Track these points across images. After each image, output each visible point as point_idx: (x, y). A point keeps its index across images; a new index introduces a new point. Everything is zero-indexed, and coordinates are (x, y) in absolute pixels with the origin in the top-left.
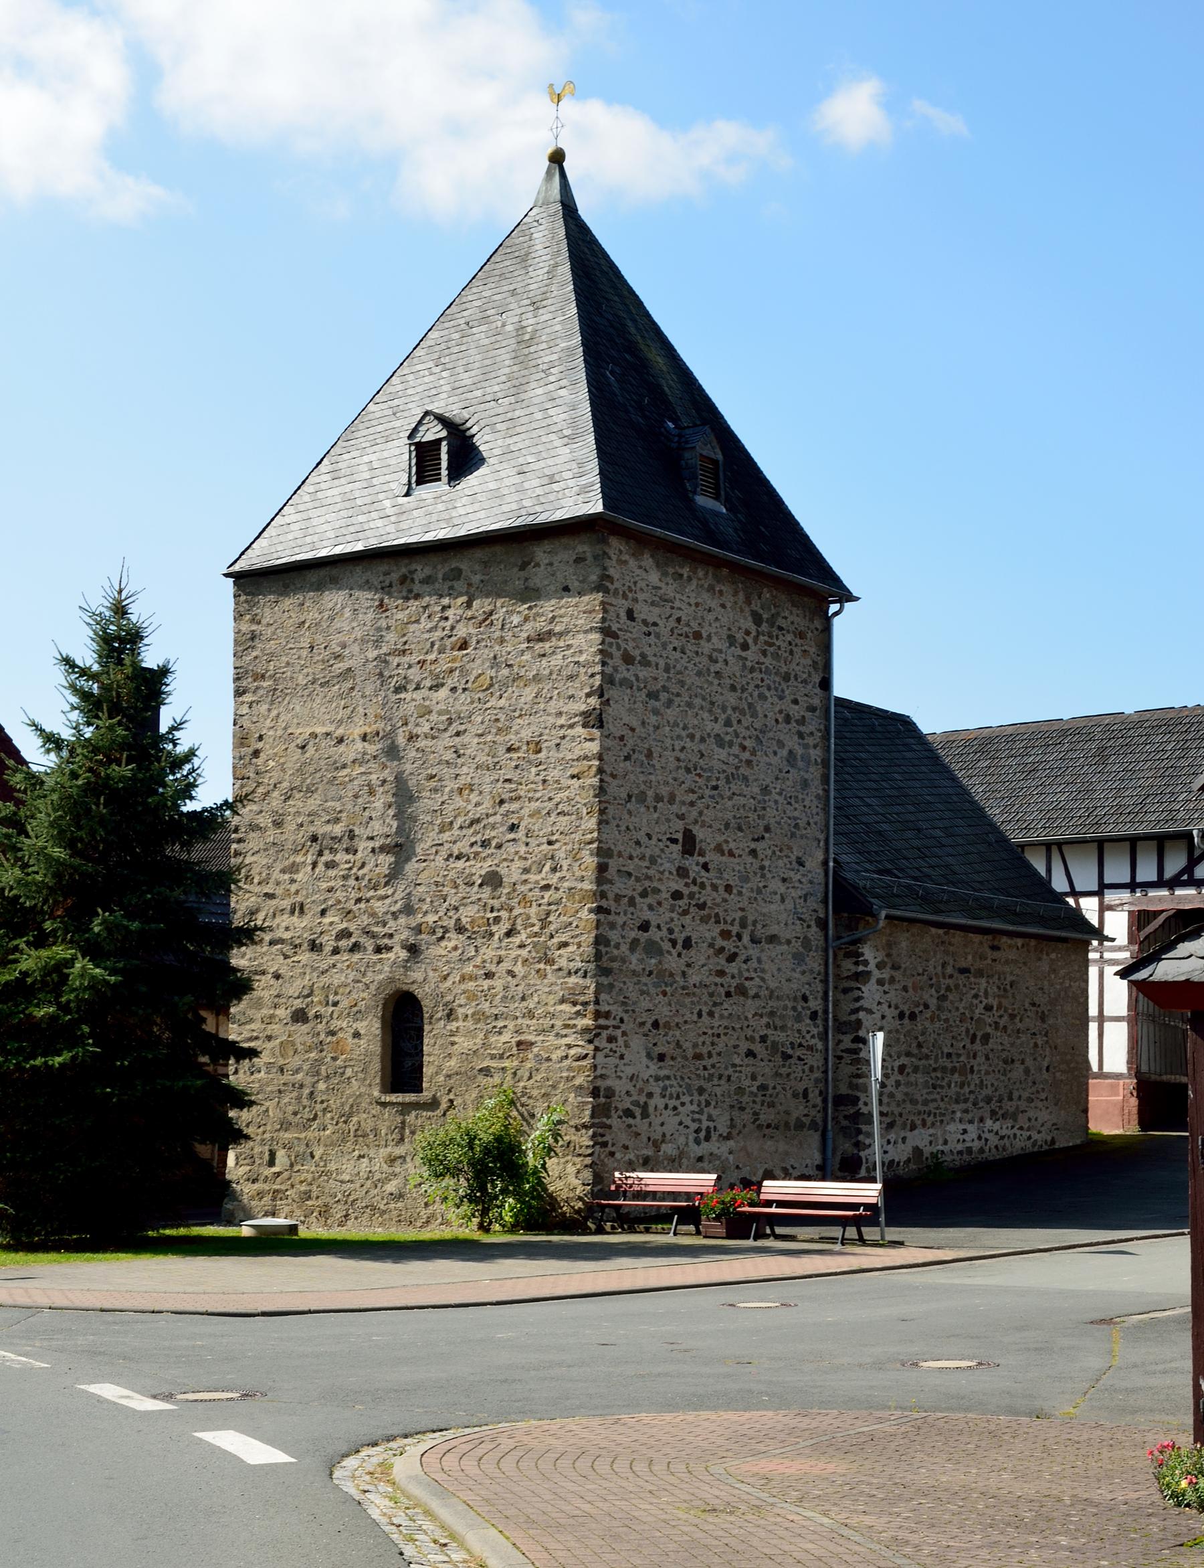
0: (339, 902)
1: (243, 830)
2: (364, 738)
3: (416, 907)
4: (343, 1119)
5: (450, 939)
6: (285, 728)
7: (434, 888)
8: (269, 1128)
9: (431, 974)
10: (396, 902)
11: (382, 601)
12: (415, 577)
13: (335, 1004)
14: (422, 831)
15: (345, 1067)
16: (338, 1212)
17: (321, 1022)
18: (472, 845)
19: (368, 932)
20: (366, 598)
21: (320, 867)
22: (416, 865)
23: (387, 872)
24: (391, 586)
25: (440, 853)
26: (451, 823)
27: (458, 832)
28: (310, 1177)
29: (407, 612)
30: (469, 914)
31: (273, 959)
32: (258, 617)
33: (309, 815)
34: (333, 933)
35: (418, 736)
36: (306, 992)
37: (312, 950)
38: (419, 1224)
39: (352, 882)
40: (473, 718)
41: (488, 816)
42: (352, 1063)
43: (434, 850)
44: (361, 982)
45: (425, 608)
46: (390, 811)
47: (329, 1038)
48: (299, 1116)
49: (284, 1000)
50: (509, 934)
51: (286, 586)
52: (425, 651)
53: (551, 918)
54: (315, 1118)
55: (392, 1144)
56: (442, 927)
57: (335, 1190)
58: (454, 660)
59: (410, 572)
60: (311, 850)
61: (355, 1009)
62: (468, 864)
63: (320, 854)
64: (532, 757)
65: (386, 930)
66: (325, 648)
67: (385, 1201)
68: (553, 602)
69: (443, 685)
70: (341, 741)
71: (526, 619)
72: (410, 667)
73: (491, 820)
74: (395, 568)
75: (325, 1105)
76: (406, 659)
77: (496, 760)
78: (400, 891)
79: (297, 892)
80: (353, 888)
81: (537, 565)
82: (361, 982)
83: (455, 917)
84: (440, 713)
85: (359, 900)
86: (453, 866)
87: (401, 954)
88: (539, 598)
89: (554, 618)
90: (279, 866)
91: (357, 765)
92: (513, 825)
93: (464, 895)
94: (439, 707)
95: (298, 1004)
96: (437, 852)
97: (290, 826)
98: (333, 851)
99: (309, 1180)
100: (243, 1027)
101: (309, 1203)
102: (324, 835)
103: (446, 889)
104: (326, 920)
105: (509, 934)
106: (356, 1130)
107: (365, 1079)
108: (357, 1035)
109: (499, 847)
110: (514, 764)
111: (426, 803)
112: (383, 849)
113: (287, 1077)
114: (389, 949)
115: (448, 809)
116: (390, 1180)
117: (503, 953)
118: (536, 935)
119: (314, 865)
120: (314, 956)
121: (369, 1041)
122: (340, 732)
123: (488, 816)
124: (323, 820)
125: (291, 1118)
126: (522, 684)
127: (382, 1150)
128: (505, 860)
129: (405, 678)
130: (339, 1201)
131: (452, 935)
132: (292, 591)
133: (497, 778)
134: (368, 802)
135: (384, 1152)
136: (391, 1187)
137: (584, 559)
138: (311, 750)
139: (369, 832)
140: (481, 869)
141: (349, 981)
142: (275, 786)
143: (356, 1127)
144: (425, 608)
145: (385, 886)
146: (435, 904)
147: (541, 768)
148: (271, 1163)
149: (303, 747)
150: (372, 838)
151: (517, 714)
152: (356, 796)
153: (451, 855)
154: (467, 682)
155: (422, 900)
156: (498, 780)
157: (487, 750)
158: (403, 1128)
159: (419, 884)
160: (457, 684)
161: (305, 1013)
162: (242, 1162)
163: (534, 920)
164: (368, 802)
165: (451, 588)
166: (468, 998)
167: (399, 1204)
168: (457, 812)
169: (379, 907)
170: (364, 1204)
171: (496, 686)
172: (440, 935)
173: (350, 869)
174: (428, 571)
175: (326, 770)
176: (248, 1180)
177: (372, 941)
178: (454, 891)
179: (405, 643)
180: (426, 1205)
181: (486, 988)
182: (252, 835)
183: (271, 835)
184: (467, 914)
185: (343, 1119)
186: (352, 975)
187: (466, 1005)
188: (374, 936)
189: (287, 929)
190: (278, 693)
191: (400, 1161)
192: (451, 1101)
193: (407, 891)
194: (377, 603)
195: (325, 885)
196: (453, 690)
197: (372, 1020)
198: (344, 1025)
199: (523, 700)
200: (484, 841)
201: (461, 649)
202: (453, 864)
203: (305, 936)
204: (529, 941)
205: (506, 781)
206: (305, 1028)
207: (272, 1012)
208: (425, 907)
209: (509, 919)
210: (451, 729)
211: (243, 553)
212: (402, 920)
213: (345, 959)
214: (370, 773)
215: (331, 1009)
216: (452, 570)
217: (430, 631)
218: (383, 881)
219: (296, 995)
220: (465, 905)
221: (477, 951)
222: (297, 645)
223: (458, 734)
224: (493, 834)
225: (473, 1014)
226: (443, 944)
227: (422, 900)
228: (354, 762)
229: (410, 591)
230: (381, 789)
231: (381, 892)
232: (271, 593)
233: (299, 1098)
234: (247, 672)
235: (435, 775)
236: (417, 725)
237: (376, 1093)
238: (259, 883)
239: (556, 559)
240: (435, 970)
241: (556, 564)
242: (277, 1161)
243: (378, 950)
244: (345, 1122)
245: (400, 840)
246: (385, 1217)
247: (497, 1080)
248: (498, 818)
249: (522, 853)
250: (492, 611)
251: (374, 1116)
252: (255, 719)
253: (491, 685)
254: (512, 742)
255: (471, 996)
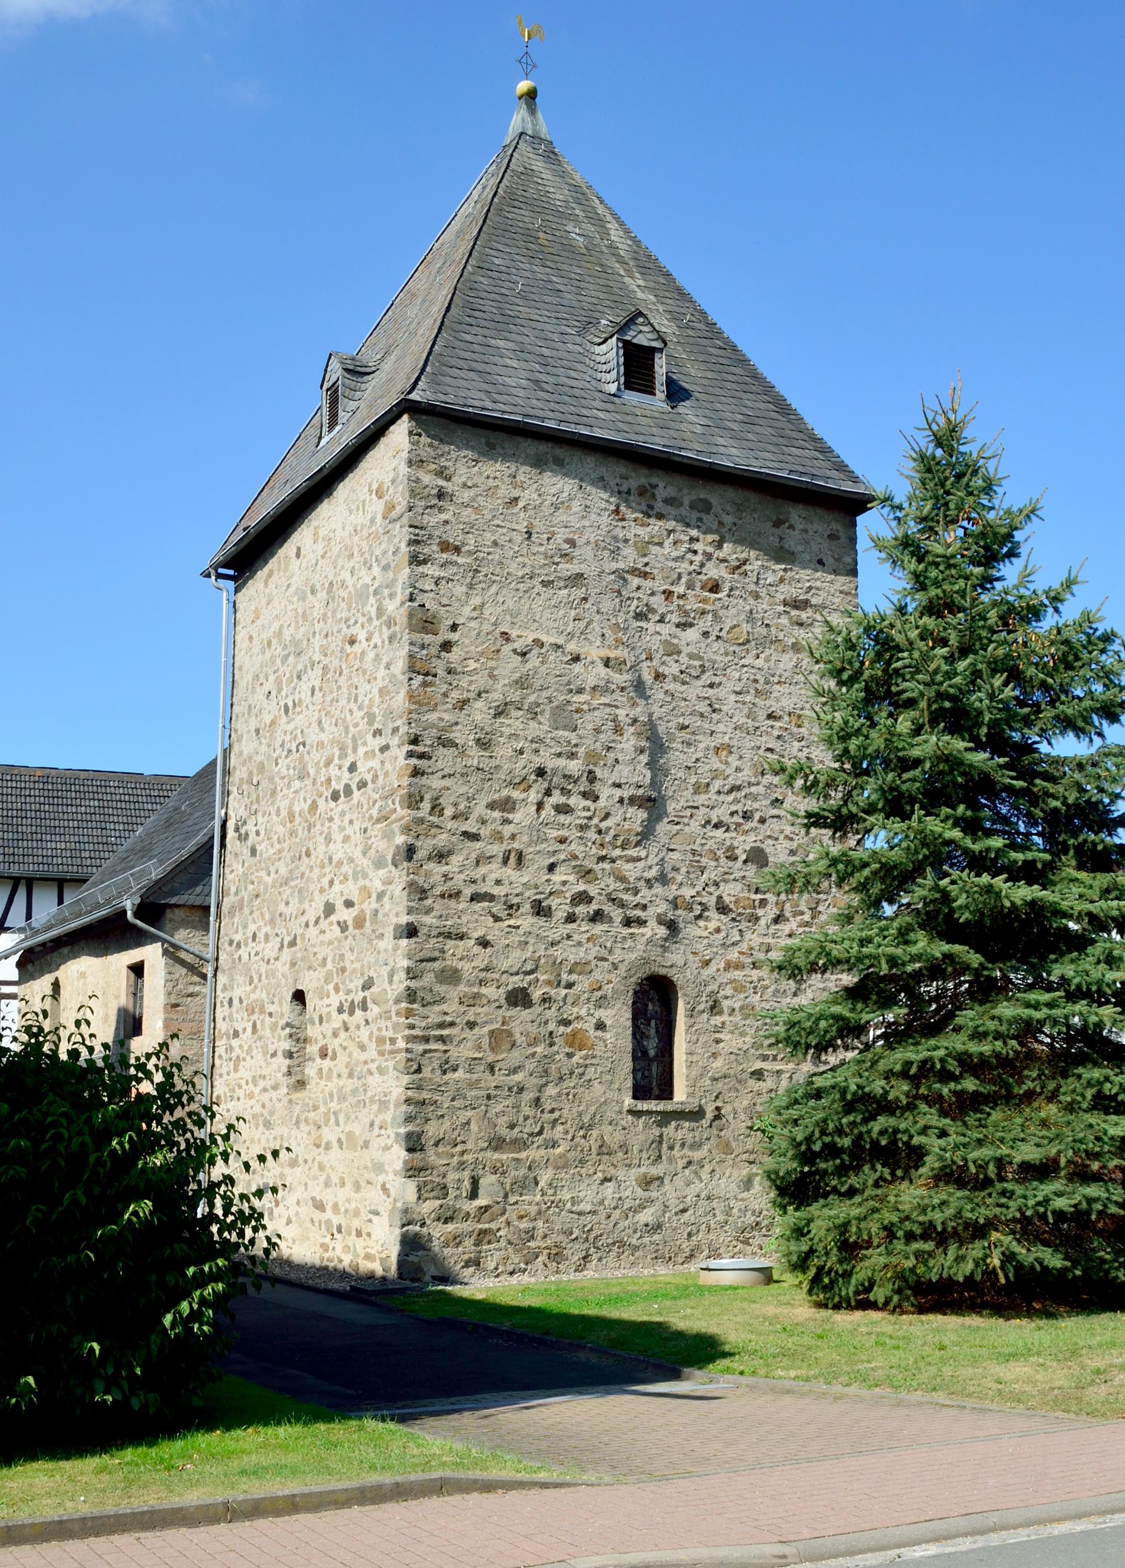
0: (576, 857)
1: (429, 743)
2: (607, 663)
3: (670, 876)
4: (582, 1133)
5: (707, 919)
6: (495, 624)
7: (690, 857)
8: (470, 1145)
9: (691, 957)
10: (650, 867)
11: (618, 506)
12: (656, 492)
13: (570, 986)
14: (674, 788)
15: (586, 1066)
16: (574, 1254)
17: (550, 1008)
18: (732, 814)
19: (614, 900)
20: (600, 498)
21: (548, 811)
22: (669, 827)
23: (640, 829)
24: (629, 492)
25: (695, 817)
26: (708, 785)
27: (715, 797)
28: (533, 1210)
29: (648, 529)
30: (732, 893)
31: (477, 921)
32: (448, 472)
33: (532, 741)
34: (568, 895)
35: (665, 676)
36: (529, 967)
37: (538, 914)
38: (680, 1260)
39: (592, 835)
40: (728, 671)
41: (750, 784)
42: (594, 1061)
43: (688, 812)
44: (607, 960)
45: (670, 532)
46: (641, 757)
47: (562, 1029)
48: (517, 1130)
49: (494, 976)
50: (777, 920)
51: (491, 446)
52: (670, 580)
53: (820, 908)
54: (540, 1133)
55: (647, 1162)
56: (700, 904)
57: (569, 1225)
58: (704, 601)
59: (651, 485)
60: (535, 787)
61: (598, 994)
62: (727, 835)
63: (548, 793)
64: (795, 730)
65: (638, 899)
66: (549, 539)
67: (639, 1234)
68: (809, 572)
69: (691, 625)
70: (576, 659)
71: (782, 580)
72: (653, 594)
73: (753, 789)
74: (633, 475)
75: (556, 1114)
76: (648, 584)
77: (757, 725)
78: (652, 853)
79: (513, 837)
80: (594, 843)
81: (791, 527)
82: (607, 960)
83: (717, 894)
84: (691, 656)
85: (602, 859)
86: (711, 834)
87: (657, 931)
88: (792, 562)
89: (810, 588)
90: (484, 800)
91: (598, 694)
92: (777, 800)
93: (726, 870)
94: (690, 649)
95: (516, 982)
96: (691, 816)
97: (503, 751)
98: (565, 791)
99: (533, 1214)
100: (429, 1008)
101: (532, 1244)
102: (555, 771)
103: (703, 860)
104: (557, 878)
105: (777, 920)
106: (601, 1147)
107: (612, 1082)
108: (600, 1026)
109: (762, 821)
110: (776, 733)
111: (677, 757)
112: (632, 800)
113: (500, 1078)
114: (641, 923)
115: (703, 768)
116: (644, 1208)
117: (771, 940)
118: (807, 924)
119: (540, 806)
120: (541, 921)
121: (618, 1034)
122: (572, 647)
123: (750, 784)
124: (553, 751)
125: (504, 1132)
126: (780, 649)
127: (633, 1171)
128: (769, 837)
129: (647, 605)
130: (576, 1238)
131: (712, 914)
132: (501, 455)
133: (758, 744)
134: (614, 741)
135: (634, 1172)
136: (646, 1216)
137: (838, 538)
138: (534, 661)
139: (615, 778)
140: (744, 843)
141: (591, 957)
142: (479, 695)
143: (599, 1142)
144: (670, 532)
145: (635, 846)
146: (691, 876)
147: (803, 743)
148: (474, 1195)
149: (524, 654)
150: (619, 786)
151: (776, 679)
152: (597, 731)
153: (708, 822)
154: (721, 629)
155: (676, 869)
156: (759, 748)
157: (746, 711)
158: (660, 1143)
159: (672, 850)
160: (710, 630)
161: (528, 995)
162: (426, 1195)
163: (803, 907)
164: (614, 741)
165: (700, 520)
166: (735, 990)
167: (656, 1237)
168: (714, 774)
169: (631, 871)
170: (610, 1241)
171: (753, 643)
172: (698, 913)
173: (590, 818)
174: (671, 491)
175: (556, 690)
176: (438, 1219)
177: (621, 910)
178: (713, 863)
179: (646, 564)
180: (690, 1235)
181: (755, 979)
182: (441, 751)
183: (475, 756)
184: (730, 892)
185: (582, 1133)
186: (595, 951)
187: (733, 997)
188: (622, 905)
189: (498, 882)
190: (480, 577)
191: (657, 1183)
192: (718, 1109)
193: (660, 856)
194: (613, 508)
195: (555, 834)
196: (706, 634)
197: (620, 1009)
198: (583, 1012)
199: (781, 665)
200: (746, 813)
201: (711, 590)
202: (710, 832)
203: (527, 894)
204: (801, 930)
205: (769, 750)
206: (526, 1014)
207: (475, 990)
208: (679, 878)
209: (777, 904)
210: (704, 677)
211: (326, 370)
212: (658, 889)
213: (583, 929)
214: (617, 707)
215: (564, 992)
216: (700, 500)
217: (676, 559)
218: (634, 839)
219: (514, 969)
220: (725, 881)
221: (741, 936)
222: (508, 525)
223: (711, 686)
224: (756, 805)
225: (742, 1008)
226: (701, 923)
227: (676, 869)
228: (594, 688)
229: (651, 507)
230: (632, 729)
231: (632, 852)
232: (473, 448)
233: (517, 1107)
234: (430, 537)
235: (688, 727)
236: (663, 663)
237: (628, 1101)
238: (454, 817)
239: (811, 528)
240: (695, 953)
241: (811, 533)
242: (481, 1192)
243: (628, 922)
244: (584, 1137)
245: (654, 794)
246: (637, 1254)
247: (769, 1083)
248: (761, 789)
249: (787, 832)
250: (747, 560)
251: (624, 1129)
252: (445, 601)
253: (748, 641)
254: (773, 709)
255: (739, 988)
